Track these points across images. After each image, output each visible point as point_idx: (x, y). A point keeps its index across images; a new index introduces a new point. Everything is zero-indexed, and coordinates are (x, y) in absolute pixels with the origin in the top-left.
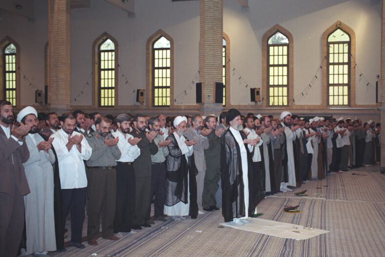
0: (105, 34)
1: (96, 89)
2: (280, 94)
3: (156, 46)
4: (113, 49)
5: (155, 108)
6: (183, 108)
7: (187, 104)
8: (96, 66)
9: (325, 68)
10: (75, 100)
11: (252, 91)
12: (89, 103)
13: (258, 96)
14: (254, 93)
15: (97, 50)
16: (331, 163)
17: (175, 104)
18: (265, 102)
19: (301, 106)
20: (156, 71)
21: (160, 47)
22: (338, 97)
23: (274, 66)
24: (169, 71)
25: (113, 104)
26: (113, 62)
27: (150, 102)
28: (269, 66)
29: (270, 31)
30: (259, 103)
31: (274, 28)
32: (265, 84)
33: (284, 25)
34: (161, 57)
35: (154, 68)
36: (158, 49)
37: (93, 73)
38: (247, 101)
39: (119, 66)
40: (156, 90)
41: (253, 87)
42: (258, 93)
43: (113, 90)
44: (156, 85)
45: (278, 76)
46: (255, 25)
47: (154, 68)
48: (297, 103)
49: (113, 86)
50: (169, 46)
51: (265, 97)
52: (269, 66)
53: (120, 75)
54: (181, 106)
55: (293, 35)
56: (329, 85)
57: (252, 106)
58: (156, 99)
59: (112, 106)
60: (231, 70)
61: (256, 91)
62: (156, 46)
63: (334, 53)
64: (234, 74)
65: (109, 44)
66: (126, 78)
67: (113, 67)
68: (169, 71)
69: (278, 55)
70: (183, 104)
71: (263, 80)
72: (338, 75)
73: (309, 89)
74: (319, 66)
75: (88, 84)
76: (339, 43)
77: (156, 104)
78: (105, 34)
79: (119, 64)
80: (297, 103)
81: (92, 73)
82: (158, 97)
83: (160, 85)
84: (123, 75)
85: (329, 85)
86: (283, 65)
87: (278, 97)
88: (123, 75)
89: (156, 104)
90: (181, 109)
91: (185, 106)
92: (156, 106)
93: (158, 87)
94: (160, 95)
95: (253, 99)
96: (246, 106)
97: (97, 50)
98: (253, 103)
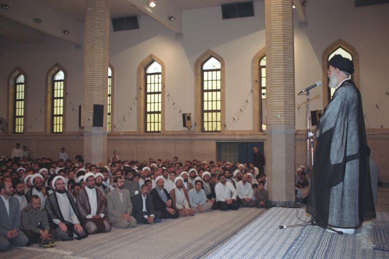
0: (56, 65)
1: (49, 116)
2: (214, 119)
3: (17, 82)
4: (63, 78)
5: (54, 134)
6: (121, 134)
7: (125, 130)
8: (49, 95)
9: (256, 92)
10: (31, 127)
11: (184, 115)
12: (42, 130)
13: (189, 121)
14: (186, 118)
15: (50, 80)
16: (336, 191)
17: (115, 130)
18: (198, 128)
19: (232, 131)
20: (149, 96)
21: (152, 72)
22: (154, 124)
23: (208, 91)
24: (62, 100)
25: (61, 131)
26: (62, 91)
27: (142, 127)
28: (203, 91)
29: (203, 56)
30: (192, 129)
31: (206, 53)
32: (199, 110)
33: (215, 50)
34: (153, 82)
35: (146, 93)
36: (151, 74)
37: (46, 101)
38: (181, 128)
39: (67, 94)
40: (148, 116)
41: (184, 113)
42: (189, 118)
43: (61, 118)
44: (148, 110)
45: (212, 101)
46: (189, 52)
47: (146, 93)
48: (229, 128)
49: (62, 113)
50: (23, 82)
51: (199, 122)
52: (203, 91)
53: (68, 102)
54: (120, 132)
55: (224, 59)
56: (146, 113)
57: (185, 131)
58: (148, 125)
59: (60, 133)
60: (166, 95)
61: (186, 116)
62: (150, 70)
63: (212, 80)
64: (168, 100)
65: (60, 76)
66: (73, 106)
67: (62, 96)
68: (62, 100)
69: (212, 80)
70: (123, 130)
71: (196, 105)
72: (154, 103)
73: (241, 114)
74: (250, 90)
75: (41, 111)
76: (212, 70)
77: (55, 131)
78: (56, 65)
79: (68, 92)
80: (229, 128)
81: (45, 102)
82: (151, 123)
83: (153, 110)
84: (70, 103)
85: (146, 113)
86: (208, 91)
87: (212, 123)
88: (70, 103)
89: (148, 130)
90: (119, 135)
91: (124, 132)
92: (55, 133)
93: (151, 113)
94: (153, 121)
95: (185, 125)
96: (179, 131)
97: (50, 80)
98: (185, 129)
